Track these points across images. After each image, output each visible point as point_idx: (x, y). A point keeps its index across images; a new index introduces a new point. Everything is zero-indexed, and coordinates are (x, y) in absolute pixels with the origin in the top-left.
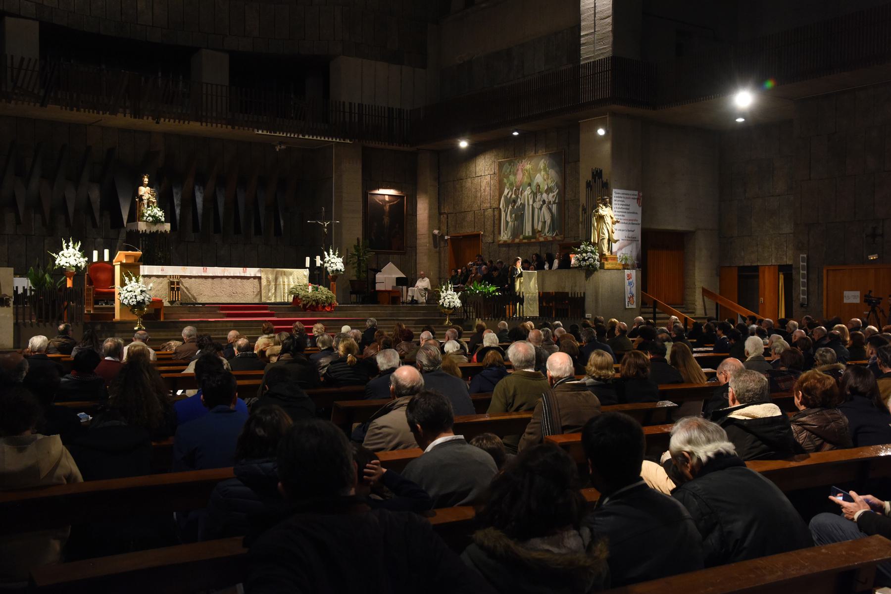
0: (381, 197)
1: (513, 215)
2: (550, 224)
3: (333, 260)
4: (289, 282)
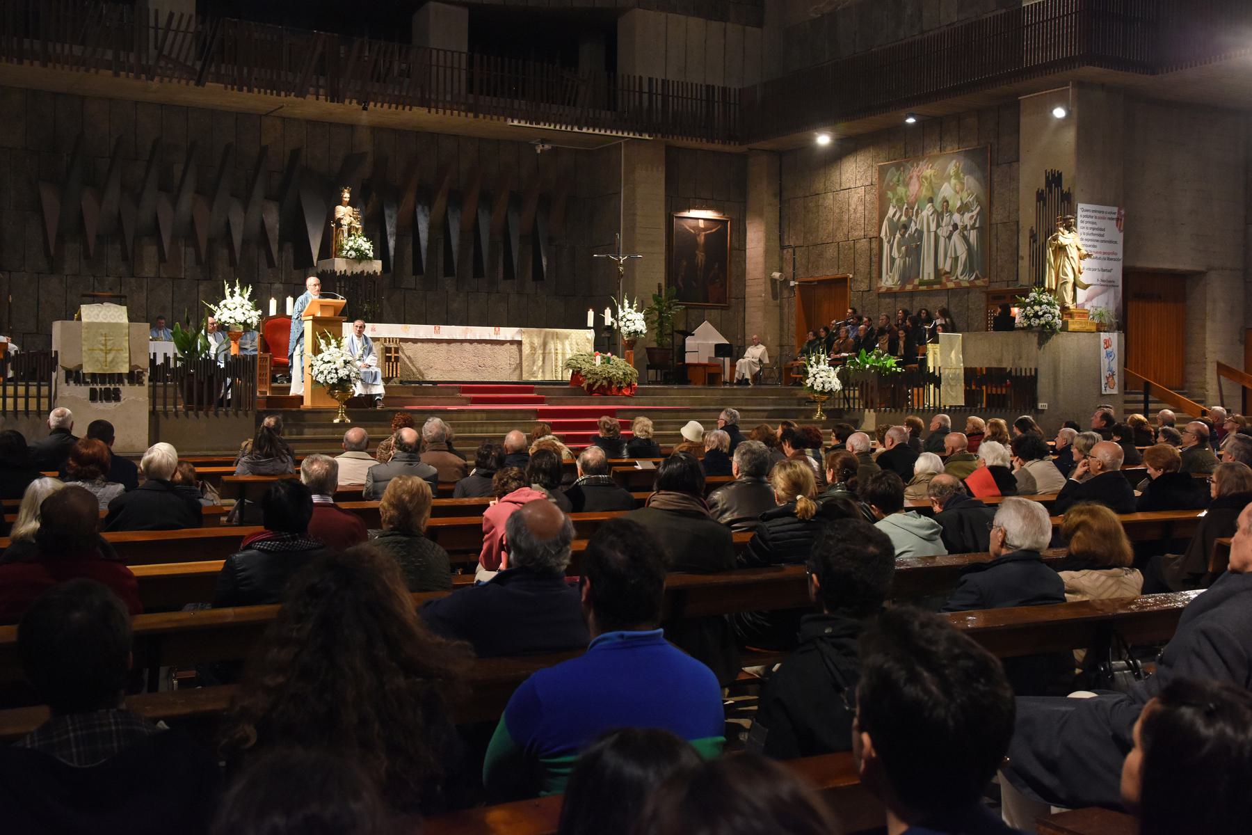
1: (903, 248)
2: (966, 259)
3: (629, 317)
4: (563, 349)
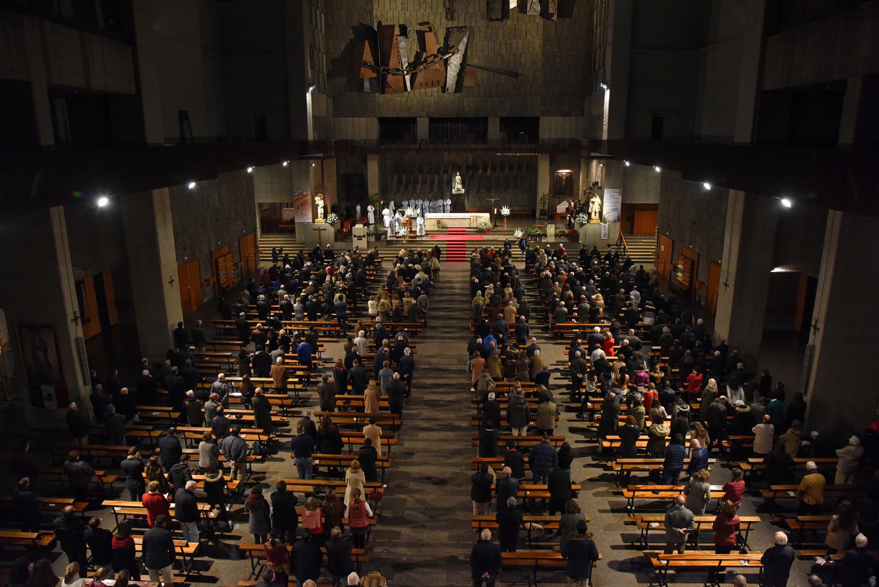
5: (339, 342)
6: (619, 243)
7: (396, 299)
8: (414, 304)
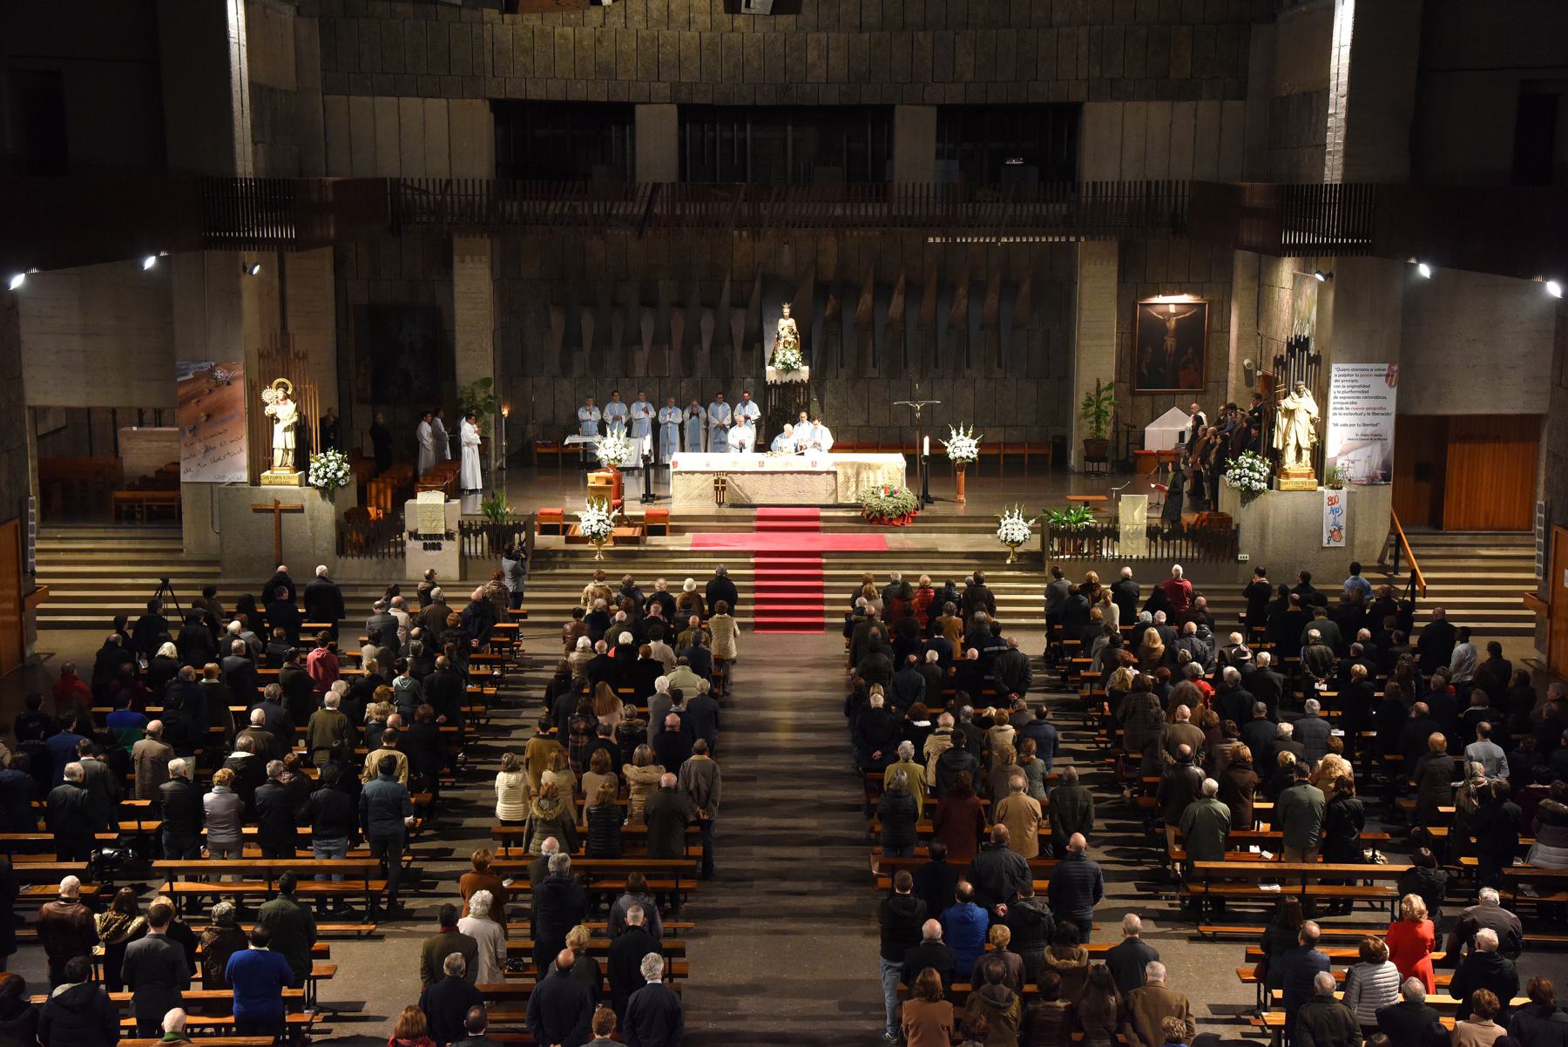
0: (1161, 309)
5: (380, 937)
6: (1389, 562)
7: (601, 772)
8: (668, 789)
